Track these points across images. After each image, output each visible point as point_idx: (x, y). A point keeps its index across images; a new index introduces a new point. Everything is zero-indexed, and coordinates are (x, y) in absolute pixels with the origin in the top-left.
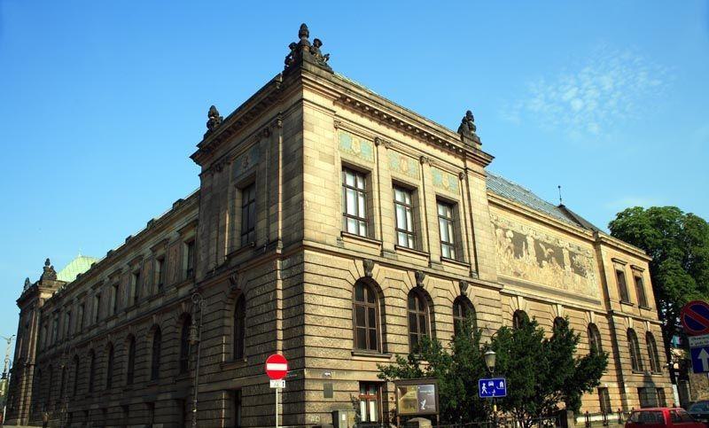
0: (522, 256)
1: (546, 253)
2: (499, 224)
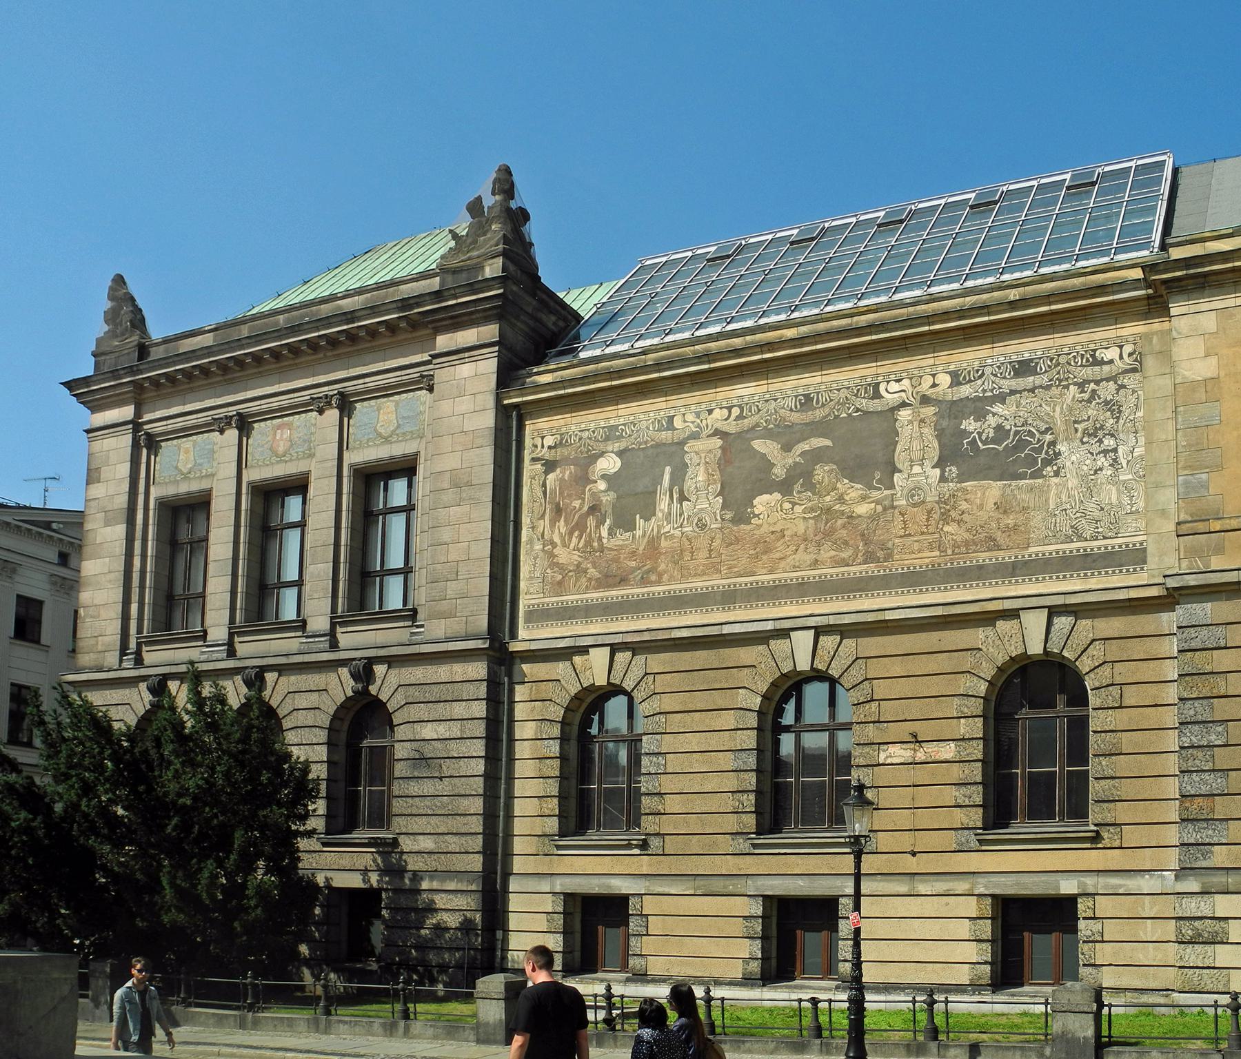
0: (649, 513)
1: (781, 463)
2: (560, 453)
